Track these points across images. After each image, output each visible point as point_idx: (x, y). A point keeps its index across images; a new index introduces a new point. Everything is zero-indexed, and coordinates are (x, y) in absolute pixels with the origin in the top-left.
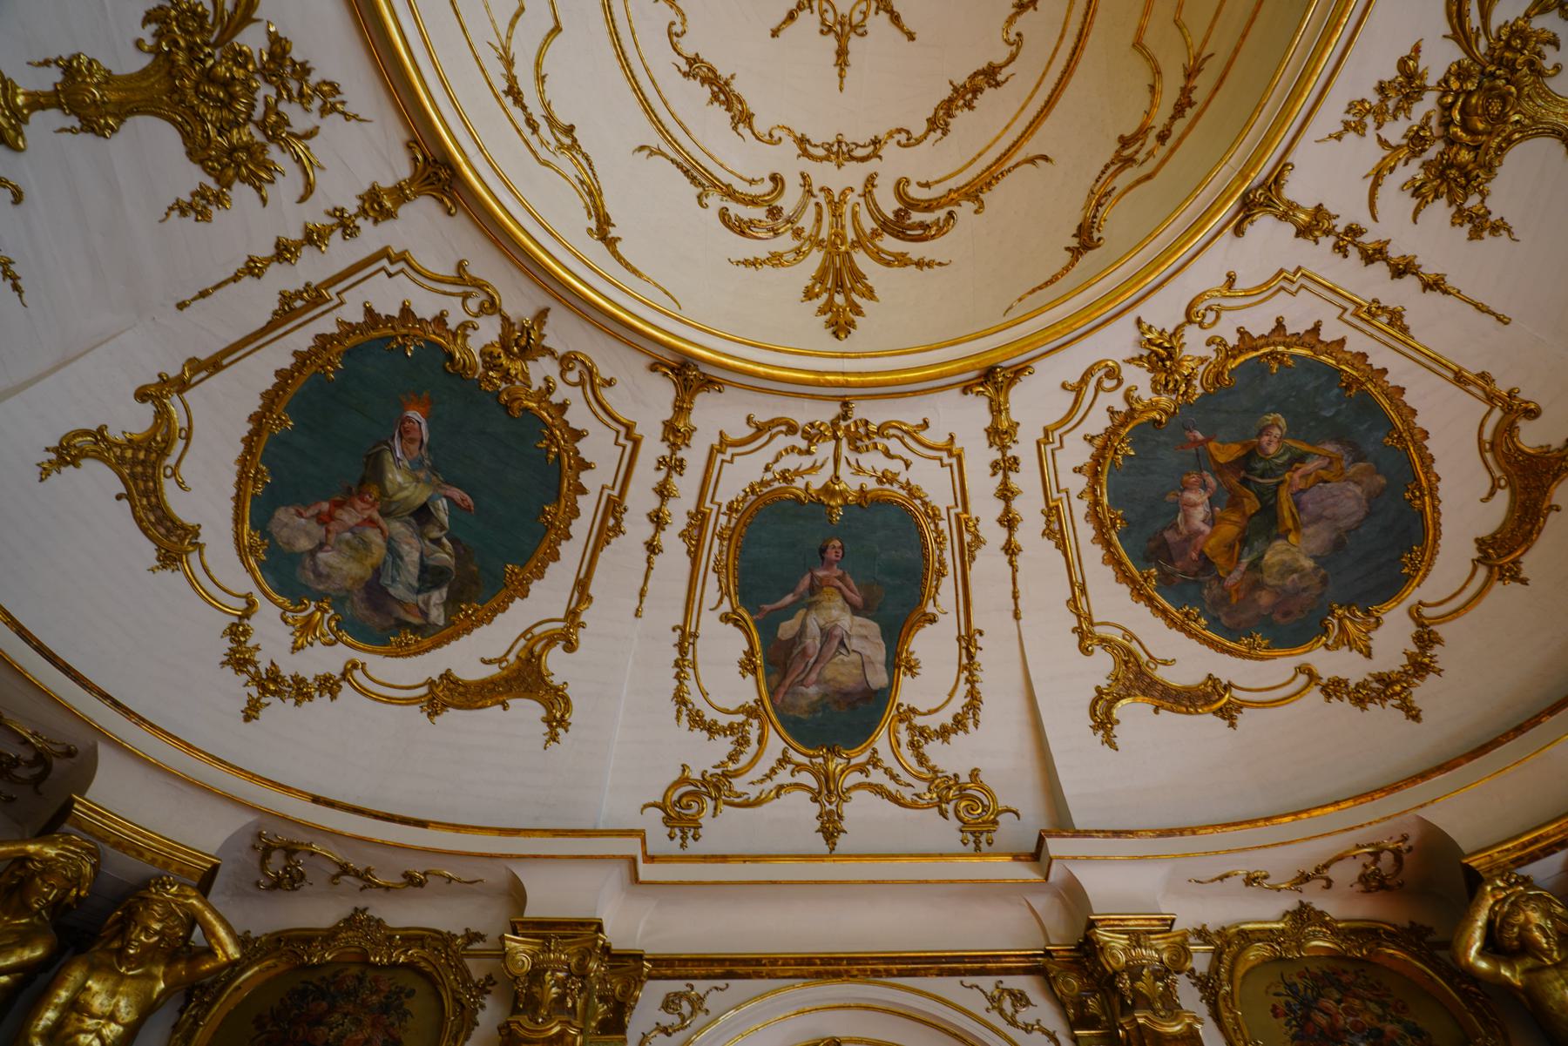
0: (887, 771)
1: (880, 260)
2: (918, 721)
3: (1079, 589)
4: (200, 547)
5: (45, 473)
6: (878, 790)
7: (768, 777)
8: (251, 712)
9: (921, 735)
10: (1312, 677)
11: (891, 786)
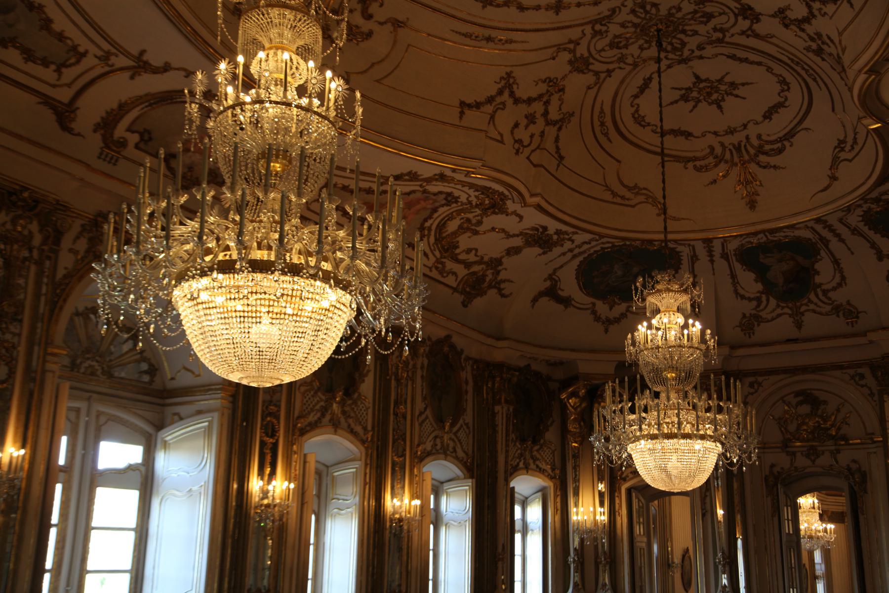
0: (816, 304)
1: (760, 166)
2: (824, 287)
3: (873, 245)
4: (573, 299)
5: (533, 307)
6: (814, 311)
7: (771, 312)
8: (606, 331)
11: (818, 309)
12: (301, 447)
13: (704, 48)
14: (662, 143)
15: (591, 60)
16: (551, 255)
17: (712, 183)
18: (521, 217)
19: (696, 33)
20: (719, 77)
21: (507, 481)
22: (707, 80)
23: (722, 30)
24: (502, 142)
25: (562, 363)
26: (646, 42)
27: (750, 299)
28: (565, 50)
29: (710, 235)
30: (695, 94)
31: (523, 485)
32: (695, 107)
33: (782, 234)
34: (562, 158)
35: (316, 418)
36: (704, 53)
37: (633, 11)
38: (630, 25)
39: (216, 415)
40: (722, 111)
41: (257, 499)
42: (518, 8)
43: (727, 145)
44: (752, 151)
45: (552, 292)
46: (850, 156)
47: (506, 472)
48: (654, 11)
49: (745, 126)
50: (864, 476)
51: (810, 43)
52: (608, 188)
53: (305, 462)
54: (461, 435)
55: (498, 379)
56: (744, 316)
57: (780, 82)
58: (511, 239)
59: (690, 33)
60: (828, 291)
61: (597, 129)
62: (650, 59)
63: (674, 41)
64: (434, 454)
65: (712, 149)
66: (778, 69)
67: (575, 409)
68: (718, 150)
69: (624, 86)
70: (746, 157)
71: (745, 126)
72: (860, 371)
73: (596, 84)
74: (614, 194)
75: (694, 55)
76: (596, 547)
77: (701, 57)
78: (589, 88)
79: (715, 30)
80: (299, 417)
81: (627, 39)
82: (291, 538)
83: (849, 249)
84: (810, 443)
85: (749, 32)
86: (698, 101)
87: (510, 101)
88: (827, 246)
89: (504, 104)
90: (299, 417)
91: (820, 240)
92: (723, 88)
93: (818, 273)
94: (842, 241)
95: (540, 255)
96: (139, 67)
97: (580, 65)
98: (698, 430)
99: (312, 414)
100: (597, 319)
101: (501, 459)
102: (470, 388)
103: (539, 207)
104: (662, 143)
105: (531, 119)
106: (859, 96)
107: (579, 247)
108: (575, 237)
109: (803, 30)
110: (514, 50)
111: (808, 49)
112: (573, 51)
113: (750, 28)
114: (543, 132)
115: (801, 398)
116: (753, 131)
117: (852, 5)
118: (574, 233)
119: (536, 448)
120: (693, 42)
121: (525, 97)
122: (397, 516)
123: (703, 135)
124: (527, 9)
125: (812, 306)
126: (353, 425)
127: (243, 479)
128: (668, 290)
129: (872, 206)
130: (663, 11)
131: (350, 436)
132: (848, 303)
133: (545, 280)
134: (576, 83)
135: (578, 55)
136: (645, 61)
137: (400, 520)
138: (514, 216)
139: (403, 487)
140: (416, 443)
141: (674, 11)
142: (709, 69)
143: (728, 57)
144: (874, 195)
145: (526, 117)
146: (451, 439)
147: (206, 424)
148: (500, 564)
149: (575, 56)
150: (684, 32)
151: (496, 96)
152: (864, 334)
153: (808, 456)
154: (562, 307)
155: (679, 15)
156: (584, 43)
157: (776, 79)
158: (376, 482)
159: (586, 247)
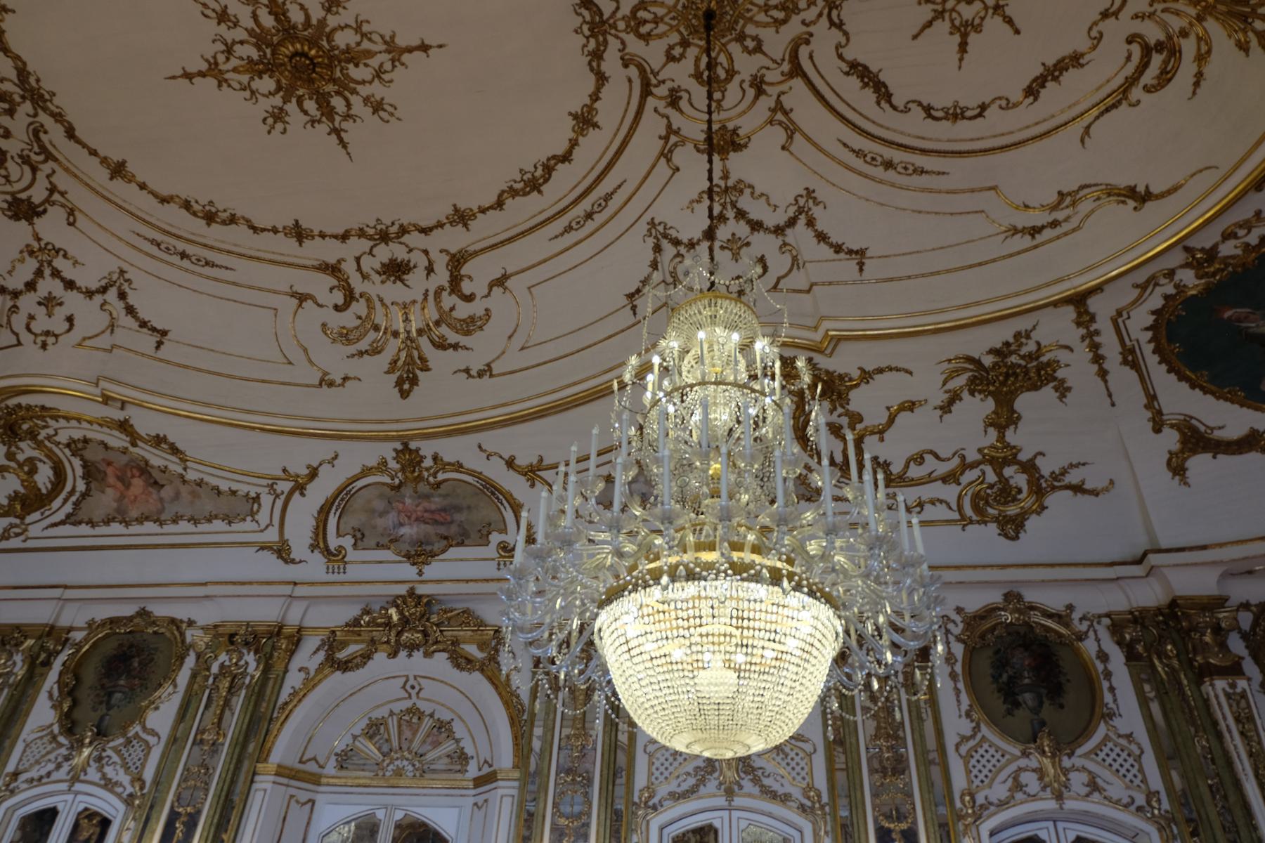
109: (39, 273)
117: (158, 348)
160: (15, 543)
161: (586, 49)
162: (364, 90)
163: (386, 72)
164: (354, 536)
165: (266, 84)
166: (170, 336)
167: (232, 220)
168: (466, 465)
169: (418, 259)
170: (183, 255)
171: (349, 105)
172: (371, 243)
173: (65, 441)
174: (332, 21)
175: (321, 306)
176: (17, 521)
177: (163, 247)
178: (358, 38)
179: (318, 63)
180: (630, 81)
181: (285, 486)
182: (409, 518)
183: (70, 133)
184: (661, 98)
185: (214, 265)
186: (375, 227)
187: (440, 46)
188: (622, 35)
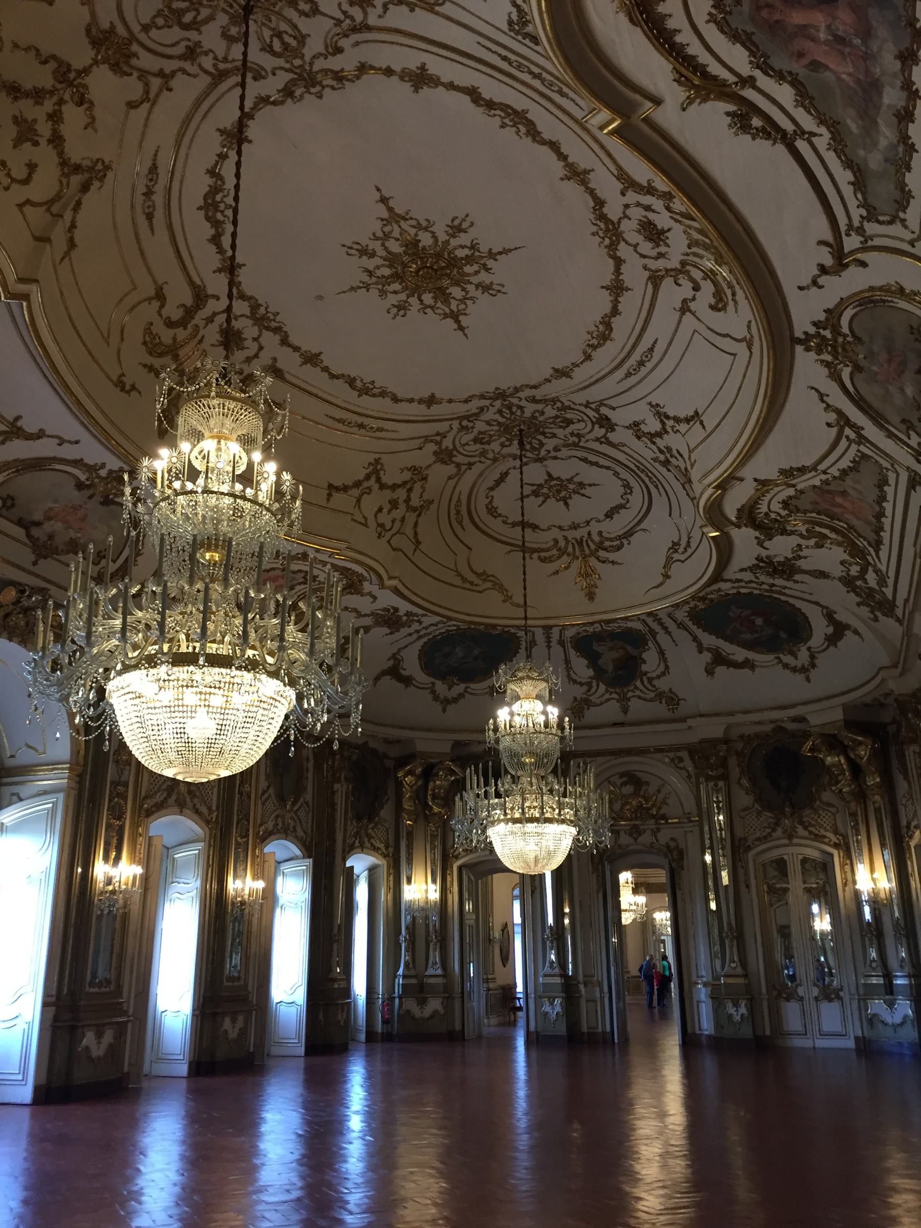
1: (600, 561)
2: (649, 675)
3: (695, 639)
6: (639, 697)
7: (601, 697)
8: (444, 710)
9: (650, 680)
10: (780, 661)
11: (643, 695)
12: (147, 829)
13: (560, 450)
14: (523, 537)
15: (455, 453)
16: (397, 635)
17: (555, 573)
18: (375, 598)
19: (554, 436)
20: (568, 477)
21: (344, 860)
22: (558, 479)
23: (579, 436)
24: (366, 525)
25: (399, 741)
26: (508, 440)
27: (581, 684)
28: (432, 441)
29: (551, 622)
30: (545, 490)
31: (360, 863)
32: (543, 502)
33: (616, 625)
34: (418, 543)
35: (162, 798)
36: (558, 454)
37: (500, 412)
38: (495, 423)
39: (61, 796)
40: (568, 508)
41: (101, 885)
42: (392, 399)
43: (570, 539)
44: (593, 547)
45: (394, 671)
46: (682, 557)
47: (344, 851)
48: (519, 413)
49: (588, 523)
50: (681, 853)
51: (658, 454)
52: (459, 574)
53: (150, 845)
54: (301, 814)
55: (338, 757)
56: (575, 699)
57: (624, 486)
58: (362, 619)
59: (549, 435)
60: (653, 678)
61: (453, 516)
62: (510, 455)
63: (534, 441)
64: (275, 834)
65: (556, 541)
66: (624, 474)
67: (411, 787)
68: (562, 543)
69: (482, 479)
70: (587, 552)
71: (588, 523)
72: (679, 754)
73: (456, 475)
74: (464, 580)
75: (551, 455)
76: (427, 925)
77: (556, 458)
78: (450, 478)
79: (572, 434)
80: (146, 798)
81: (491, 436)
82: (133, 927)
83: (674, 641)
84: (633, 823)
85: (603, 440)
86: (547, 497)
87: (376, 487)
88: (654, 638)
89: (370, 488)
90: (146, 798)
91: (650, 632)
92: (571, 486)
93: (645, 662)
94: (669, 633)
95: (387, 635)
96: (12, 432)
97: (444, 456)
98: (543, 813)
99: (159, 794)
100: (436, 698)
101: (339, 837)
102: (311, 765)
103: (396, 591)
104: (523, 537)
105: (394, 504)
106: (704, 508)
107: (426, 628)
108: (423, 619)
109: (654, 443)
110: (384, 439)
111: (655, 460)
112: (439, 443)
113: (604, 436)
114: (404, 518)
115: (625, 779)
116: (594, 528)
117: (704, 427)
118: (423, 615)
119: (371, 826)
120: (550, 444)
121: (390, 483)
122: (239, 899)
123: (549, 529)
124: (401, 401)
125: (638, 693)
126: (198, 806)
127: (88, 864)
128: (529, 678)
129: (698, 604)
130: (528, 414)
131: (196, 817)
132: (670, 691)
133: (389, 659)
134: (440, 473)
135: (443, 447)
136: (504, 457)
137: (243, 903)
138: (368, 597)
139: (246, 869)
140: (259, 822)
141: (537, 414)
142: (562, 469)
143: (580, 459)
144: (701, 595)
145: (390, 502)
146: (291, 818)
147: (50, 805)
148: (335, 946)
149: (440, 448)
150: (544, 434)
151: (364, 481)
152: (683, 720)
153: (631, 835)
154: (402, 686)
155: (541, 418)
156: (450, 436)
157: (621, 483)
158: (219, 865)
159: (433, 628)
160: (890, 582)
161: (336, 86)
162: (442, 237)
163: (419, 223)
164: (908, 428)
165: (456, 292)
166: (700, 412)
167: (609, 326)
168: (831, 306)
169: (636, 213)
170: (641, 363)
171: (463, 247)
172: (622, 244)
173: (786, 512)
174: (381, 252)
175: (694, 299)
176: (870, 569)
177: (631, 371)
178: (392, 240)
179: (422, 264)
180: (357, 44)
181: (848, 431)
182: (894, 379)
183: (535, 387)
184: (365, 13)
185: (651, 350)
186: (603, 238)
187: (378, 190)
188: (307, 58)
